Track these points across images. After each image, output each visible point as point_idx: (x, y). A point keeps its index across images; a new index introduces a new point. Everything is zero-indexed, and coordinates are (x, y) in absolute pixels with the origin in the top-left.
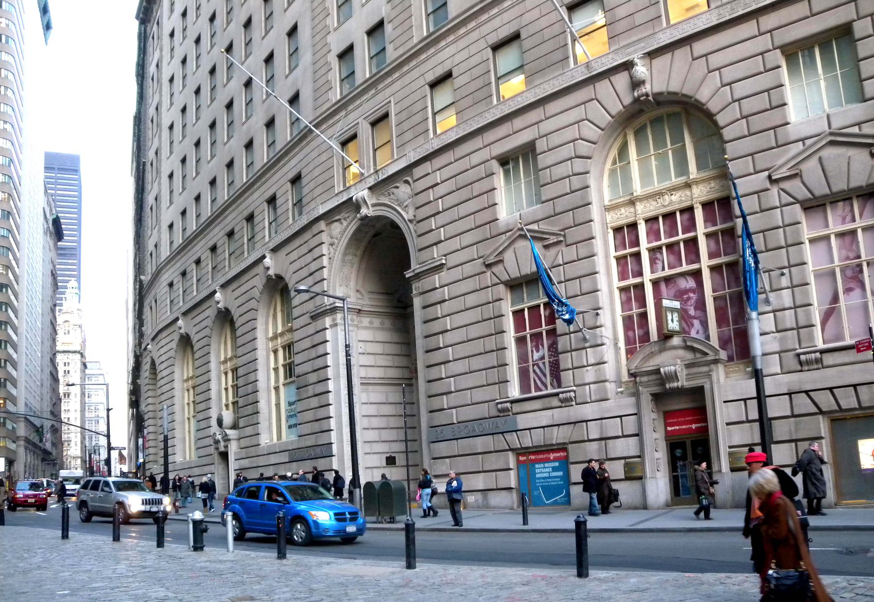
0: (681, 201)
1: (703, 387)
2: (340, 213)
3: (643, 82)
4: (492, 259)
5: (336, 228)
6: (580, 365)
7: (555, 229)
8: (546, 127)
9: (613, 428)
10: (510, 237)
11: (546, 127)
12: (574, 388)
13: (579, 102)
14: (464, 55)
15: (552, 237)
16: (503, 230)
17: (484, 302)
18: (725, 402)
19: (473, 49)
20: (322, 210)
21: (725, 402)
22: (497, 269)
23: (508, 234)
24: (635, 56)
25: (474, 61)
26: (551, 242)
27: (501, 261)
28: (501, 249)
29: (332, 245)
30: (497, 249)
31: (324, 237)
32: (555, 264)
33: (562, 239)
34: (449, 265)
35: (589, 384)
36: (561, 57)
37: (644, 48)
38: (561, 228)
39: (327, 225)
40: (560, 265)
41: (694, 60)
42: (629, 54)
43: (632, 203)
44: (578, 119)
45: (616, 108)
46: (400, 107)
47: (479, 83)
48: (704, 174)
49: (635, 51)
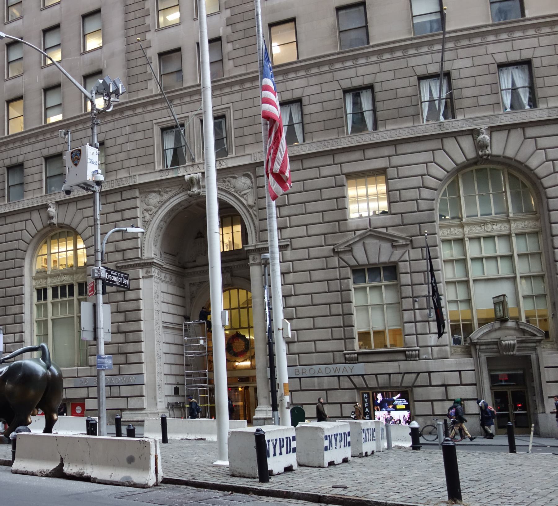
0: (501, 230)
1: (530, 356)
2: (158, 186)
3: (487, 147)
4: (342, 248)
5: (154, 199)
6: (423, 332)
7: (403, 235)
8: (396, 161)
9: (453, 378)
10: (360, 235)
11: (396, 161)
12: (418, 348)
13: (429, 149)
14: (317, 89)
15: (401, 241)
16: (354, 228)
17: (333, 278)
18: (545, 367)
19: (326, 87)
20: (139, 180)
21: (545, 367)
22: (347, 257)
23: (358, 233)
24: (482, 127)
25: (325, 97)
26: (401, 244)
27: (351, 251)
28: (351, 242)
29: (147, 210)
30: (348, 241)
31: (138, 202)
32: (402, 259)
33: (409, 243)
34: (294, 246)
35: (431, 346)
36: (413, 113)
37: (489, 123)
38: (409, 235)
39: (140, 193)
40: (407, 261)
41: (525, 139)
42: (477, 124)
43: (462, 226)
44: (427, 160)
45: (460, 159)
46: (238, 115)
47: (332, 115)
48: (520, 216)
49: (482, 124)
